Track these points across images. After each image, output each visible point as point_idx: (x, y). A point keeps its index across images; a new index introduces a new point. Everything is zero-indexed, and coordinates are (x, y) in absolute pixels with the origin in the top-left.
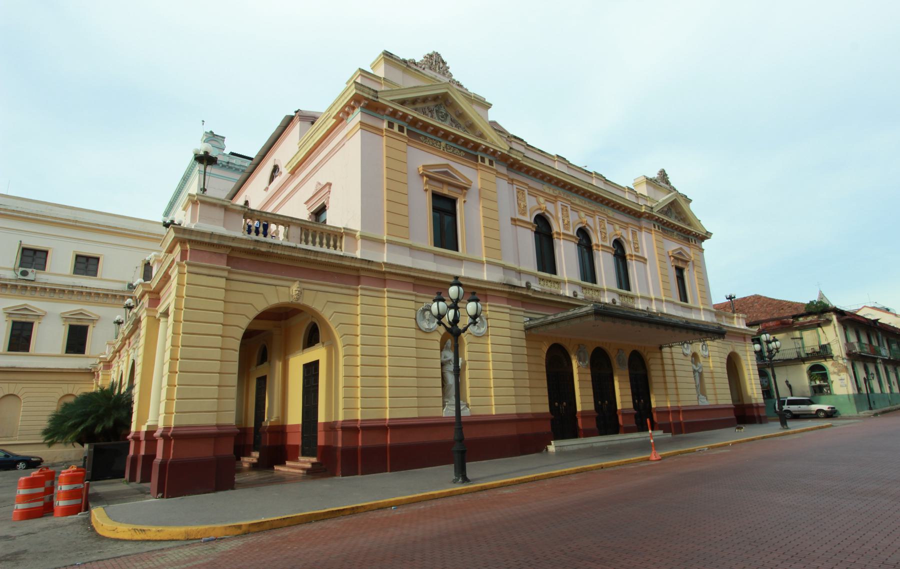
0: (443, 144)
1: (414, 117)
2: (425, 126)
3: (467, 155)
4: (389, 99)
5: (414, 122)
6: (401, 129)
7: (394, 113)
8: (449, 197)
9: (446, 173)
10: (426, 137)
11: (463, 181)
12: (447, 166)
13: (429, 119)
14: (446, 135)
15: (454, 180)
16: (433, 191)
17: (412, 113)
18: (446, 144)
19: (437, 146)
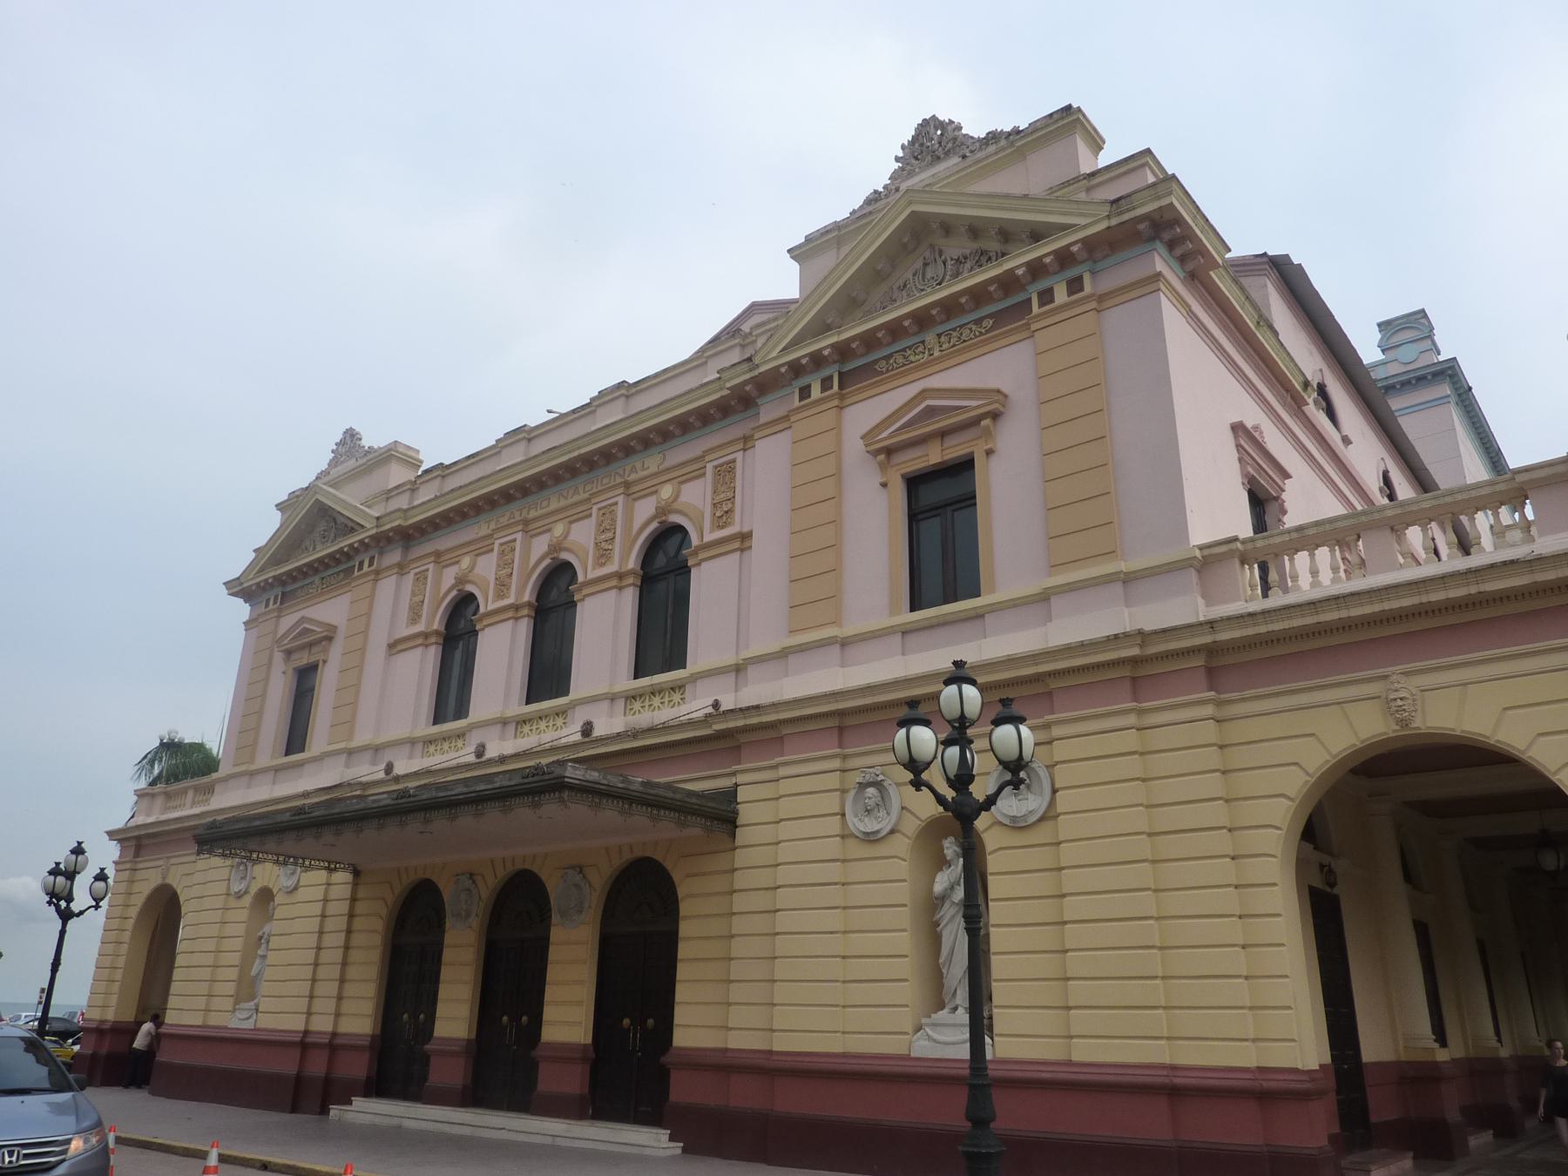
0: (930, 337)
1: (832, 346)
2: (869, 341)
3: (1000, 318)
4: (774, 354)
5: (843, 351)
6: (826, 384)
7: (796, 369)
8: (950, 464)
9: (931, 412)
10: (890, 356)
11: (974, 403)
12: (924, 394)
14: (922, 320)
15: (957, 415)
16: (902, 476)
18: (939, 336)
19: (921, 356)
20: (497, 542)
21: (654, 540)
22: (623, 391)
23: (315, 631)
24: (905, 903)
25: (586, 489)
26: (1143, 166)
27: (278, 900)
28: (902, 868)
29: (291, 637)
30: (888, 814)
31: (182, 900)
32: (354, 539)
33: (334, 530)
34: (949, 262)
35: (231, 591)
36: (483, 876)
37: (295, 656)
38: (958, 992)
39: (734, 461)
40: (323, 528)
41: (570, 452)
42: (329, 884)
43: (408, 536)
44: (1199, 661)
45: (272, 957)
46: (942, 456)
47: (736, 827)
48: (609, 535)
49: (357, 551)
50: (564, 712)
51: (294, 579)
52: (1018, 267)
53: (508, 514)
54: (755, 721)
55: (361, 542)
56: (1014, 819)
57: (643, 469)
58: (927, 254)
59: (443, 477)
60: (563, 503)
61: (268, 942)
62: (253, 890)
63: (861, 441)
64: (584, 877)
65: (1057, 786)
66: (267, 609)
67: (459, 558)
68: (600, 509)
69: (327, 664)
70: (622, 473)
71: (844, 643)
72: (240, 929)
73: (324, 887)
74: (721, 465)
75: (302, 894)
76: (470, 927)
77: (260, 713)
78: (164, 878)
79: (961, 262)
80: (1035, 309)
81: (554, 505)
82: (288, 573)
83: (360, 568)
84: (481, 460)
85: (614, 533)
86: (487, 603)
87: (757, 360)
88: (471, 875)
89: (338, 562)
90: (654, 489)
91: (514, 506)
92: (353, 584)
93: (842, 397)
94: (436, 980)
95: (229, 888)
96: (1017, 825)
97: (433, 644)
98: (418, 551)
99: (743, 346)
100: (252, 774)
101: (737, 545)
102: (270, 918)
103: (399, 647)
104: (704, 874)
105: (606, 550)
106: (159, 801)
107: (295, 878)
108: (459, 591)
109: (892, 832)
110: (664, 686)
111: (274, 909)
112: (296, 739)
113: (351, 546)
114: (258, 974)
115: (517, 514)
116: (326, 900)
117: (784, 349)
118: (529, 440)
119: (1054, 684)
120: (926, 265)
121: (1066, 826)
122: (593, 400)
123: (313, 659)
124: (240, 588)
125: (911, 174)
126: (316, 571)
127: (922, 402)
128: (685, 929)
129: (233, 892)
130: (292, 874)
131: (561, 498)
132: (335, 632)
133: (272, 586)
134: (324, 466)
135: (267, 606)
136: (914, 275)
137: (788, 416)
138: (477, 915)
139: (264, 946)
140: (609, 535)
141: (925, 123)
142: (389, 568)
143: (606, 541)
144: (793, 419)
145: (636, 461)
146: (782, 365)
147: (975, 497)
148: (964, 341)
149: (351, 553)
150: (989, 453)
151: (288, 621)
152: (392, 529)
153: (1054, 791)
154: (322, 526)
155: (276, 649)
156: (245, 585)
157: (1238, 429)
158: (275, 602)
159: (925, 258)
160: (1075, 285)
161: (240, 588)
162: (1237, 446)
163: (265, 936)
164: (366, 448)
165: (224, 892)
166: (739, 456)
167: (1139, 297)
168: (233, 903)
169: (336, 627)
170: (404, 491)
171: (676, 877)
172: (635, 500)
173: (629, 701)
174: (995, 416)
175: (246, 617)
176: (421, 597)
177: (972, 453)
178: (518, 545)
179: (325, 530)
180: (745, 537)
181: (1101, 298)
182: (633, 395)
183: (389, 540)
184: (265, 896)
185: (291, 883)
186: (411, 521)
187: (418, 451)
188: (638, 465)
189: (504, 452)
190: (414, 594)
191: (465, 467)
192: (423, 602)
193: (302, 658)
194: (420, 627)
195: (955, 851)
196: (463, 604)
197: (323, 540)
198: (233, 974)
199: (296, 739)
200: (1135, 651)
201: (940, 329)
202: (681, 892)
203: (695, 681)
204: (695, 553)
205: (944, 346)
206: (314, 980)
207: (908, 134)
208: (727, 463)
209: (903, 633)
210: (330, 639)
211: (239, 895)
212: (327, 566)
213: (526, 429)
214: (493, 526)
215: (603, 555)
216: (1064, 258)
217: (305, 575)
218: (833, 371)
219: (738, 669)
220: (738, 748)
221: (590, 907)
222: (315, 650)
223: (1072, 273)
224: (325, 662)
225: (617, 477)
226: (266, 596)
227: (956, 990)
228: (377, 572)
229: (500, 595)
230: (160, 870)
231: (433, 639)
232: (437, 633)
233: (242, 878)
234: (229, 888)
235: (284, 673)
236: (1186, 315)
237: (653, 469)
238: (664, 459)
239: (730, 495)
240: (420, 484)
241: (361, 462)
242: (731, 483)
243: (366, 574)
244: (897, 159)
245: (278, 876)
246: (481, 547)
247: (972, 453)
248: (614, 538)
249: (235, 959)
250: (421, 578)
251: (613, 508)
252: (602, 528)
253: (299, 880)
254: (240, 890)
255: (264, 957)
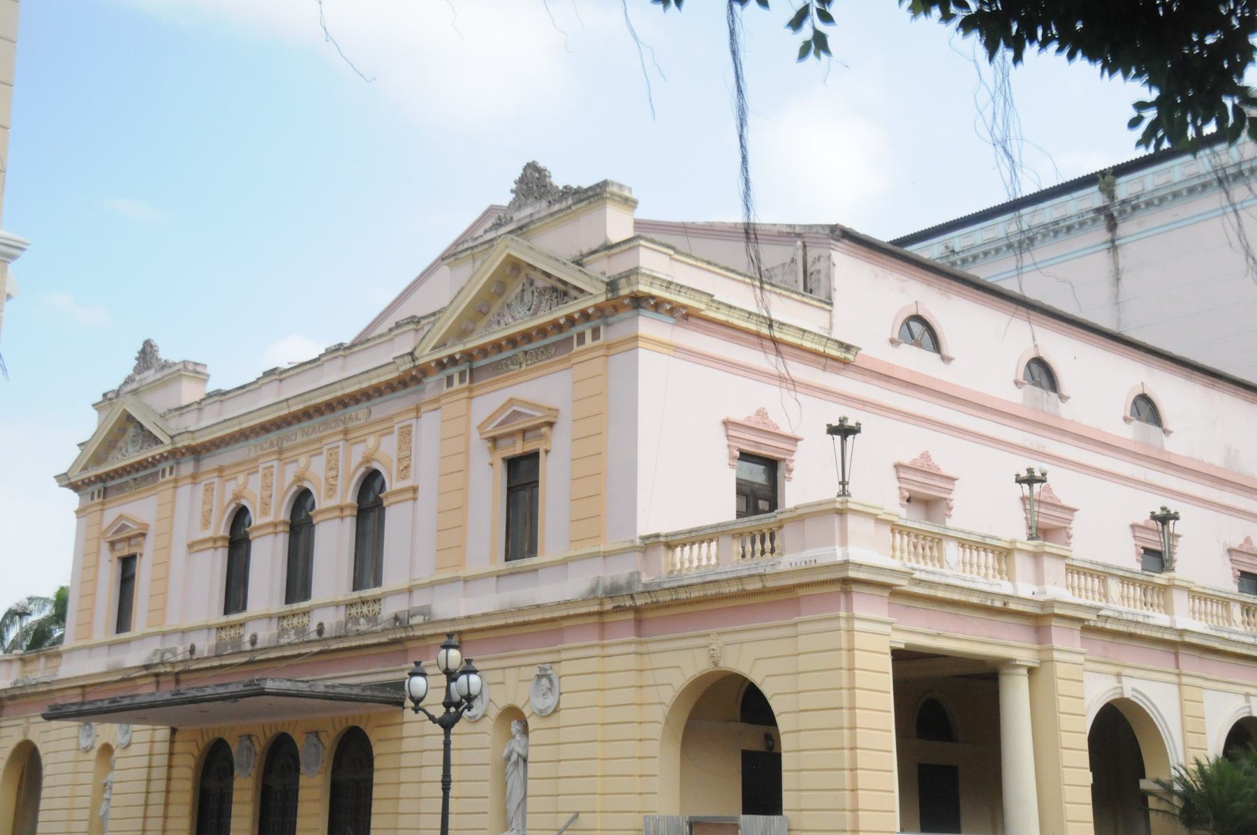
2: (484, 351)
4: (427, 351)
5: (469, 356)
7: (441, 365)
9: (516, 414)
11: (538, 414)
12: (511, 401)
13: (498, 331)
16: (504, 459)
17: (456, 349)
20: (261, 466)
21: (363, 483)
22: (341, 353)
23: (131, 528)
24: (487, 762)
25: (321, 429)
26: (640, 245)
27: (117, 753)
28: (487, 740)
29: (112, 532)
30: (482, 703)
31: (42, 752)
32: (156, 451)
33: (141, 436)
34: (536, 294)
35: (64, 483)
36: (258, 738)
37: (118, 546)
38: (514, 820)
39: (411, 426)
40: (131, 435)
41: (304, 402)
42: (153, 742)
43: (197, 452)
44: (631, 616)
45: (115, 800)
46: (523, 448)
47: (404, 708)
48: (333, 473)
49: (159, 461)
50: (308, 612)
51: (113, 478)
52: (561, 317)
53: (269, 441)
54: (411, 634)
55: (161, 455)
56: (541, 711)
57: (357, 418)
58: (524, 281)
59: (221, 401)
60: (305, 439)
61: (111, 788)
62: (98, 745)
63: (477, 430)
64: (319, 739)
65: (562, 691)
66: (93, 502)
67: (237, 475)
68: (329, 449)
69: (144, 557)
70: (343, 420)
71: (466, 580)
72: (88, 778)
73: (149, 744)
74: (403, 428)
75: (134, 750)
76: (250, 775)
77: (93, 595)
78: (25, 735)
79: (543, 294)
80: (576, 348)
81: (299, 439)
82: (107, 474)
83: (163, 475)
84: (249, 391)
85: (338, 472)
86: (256, 519)
87: (417, 354)
88: (249, 737)
89: (146, 468)
90: (363, 438)
91: (273, 436)
92: (160, 489)
93: (470, 390)
94: (229, 816)
95: (78, 743)
96: (544, 715)
97: (219, 547)
98: (209, 463)
99: (416, 330)
100: (91, 648)
101: (410, 495)
102: (111, 768)
103: (196, 548)
104: (387, 740)
105: (332, 485)
106: (17, 666)
107: (128, 736)
108: (237, 504)
109: (484, 716)
110: (368, 599)
111: (114, 761)
112: (123, 620)
113: (154, 457)
114: (104, 814)
115: (275, 442)
116: (151, 755)
117: (434, 348)
118: (281, 380)
119: (565, 624)
120: (523, 290)
121: (564, 717)
122: (321, 356)
123: (132, 551)
124: (66, 481)
125: (519, 208)
126: (129, 473)
127: (510, 407)
128: (377, 777)
129: (81, 748)
130: (126, 733)
131: (305, 435)
132: (147, 529)
133: (94, 483)
134: (129, 370)
135: (92, 498)
136: (516, 298)
137: (438, 398)
138: (254, 767)
139: (108, 792)
140: (333, 473)
141: (528, 165)
142: (185, 478)
143: (333, 478)
144: (443, 401)
145: (352, 411)
146: (432, 361)
147: (538, 481)
148: (540, 361)
149: (155, 462)
150: (547, 452)
151: (111, 514)
152: (184, 447)
153: (561, 694)
154: (131, 431)
155: (102, 541)
156: (73, 480)
157: (726, 423)
158: (99, 496)
159: (524, 285)
160: (596, 334)
161: (67, 482)
162: (728, 436)
163: (109, 784)
164: (163, 361)
165: (75, 747)
166: (414, 422)
167: (628, 350)
168: (82, 756)
169: (147, 525)
170: (193, 410)
171: (372, 739)
172: (352, 444)
173: (348, 609)
174: (550, 424)
175: (76, 506)
176: (210, 507)
177: (539, 449)
178: (275, 470)
179: (134, 436)
180: (415, 490)
181: (609, 347)
182: (348, 355)
183: (183, 454)
184: (107, 750)
185: (124, 740)
186: (199, 441)
187: (205, 366)
188: (353, 415)
189: (264, 389)
190: (204, 502)
191: (237, 396)
192: (211, 510)
193: (123, 549)
194: (209, 533)
195: (517, 729)
196: (240, 515)
197: (134, 444)
198: (85, 814)
199: (123, 620)
200: (596, 608)
201: (527, 347)
202: (375, 751)
203: (385, 597)
204: (386, 497)
205: (529, 362)
206: (145, 817)
207: (518, 173)
208: (407, 426)
209: (498, 576)
210: (143, 535)
211: (87, 750)
212: (137, 470)
213: (277, 372)
214: (259, 453)
215: (331, 489)
216: (585, 315)
217: (121, 476)
218: (465, 367)
219: (410, 591)
220: (406, 651)
221: (323, 761)
222: (133, 542)
223: (593, 323)
224: (141, 555)
225: (341, 424)
226: (90, 489)
227: (512, 818)
228: (176, 481)
229: (265, 512)
230: (21, 728)
231: (220, 543)
232: (223, 538)
233: (88, 736)
234: (78, 743)
235: (110, 561)
236: (672, 352)
237: (362, 421)
238: (370, 412)
239: (408, 453)
240: (205, 405)
241: (159, 375)
242: (409, 443)
243: (168, 482)
244: (512, 191)
245: (116, 734)
246: (250, 466)
247: (539, 449)
248: (337, 476)
249: (86, 802)
250: (209, 489)
251: (337, 450)
252: (330, 467)
253: (131, 738)
254: (87, 746)
255: (108, 800)
